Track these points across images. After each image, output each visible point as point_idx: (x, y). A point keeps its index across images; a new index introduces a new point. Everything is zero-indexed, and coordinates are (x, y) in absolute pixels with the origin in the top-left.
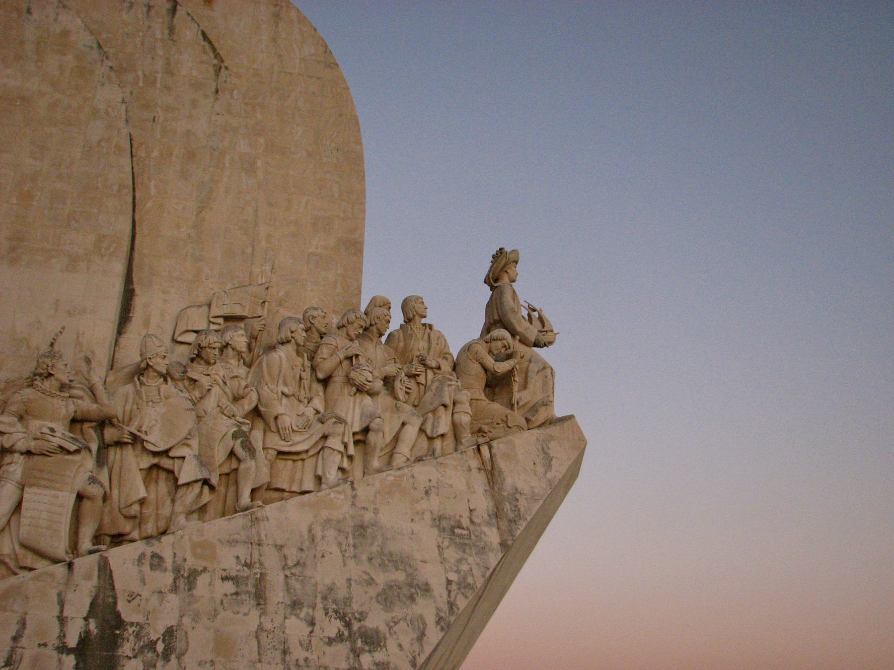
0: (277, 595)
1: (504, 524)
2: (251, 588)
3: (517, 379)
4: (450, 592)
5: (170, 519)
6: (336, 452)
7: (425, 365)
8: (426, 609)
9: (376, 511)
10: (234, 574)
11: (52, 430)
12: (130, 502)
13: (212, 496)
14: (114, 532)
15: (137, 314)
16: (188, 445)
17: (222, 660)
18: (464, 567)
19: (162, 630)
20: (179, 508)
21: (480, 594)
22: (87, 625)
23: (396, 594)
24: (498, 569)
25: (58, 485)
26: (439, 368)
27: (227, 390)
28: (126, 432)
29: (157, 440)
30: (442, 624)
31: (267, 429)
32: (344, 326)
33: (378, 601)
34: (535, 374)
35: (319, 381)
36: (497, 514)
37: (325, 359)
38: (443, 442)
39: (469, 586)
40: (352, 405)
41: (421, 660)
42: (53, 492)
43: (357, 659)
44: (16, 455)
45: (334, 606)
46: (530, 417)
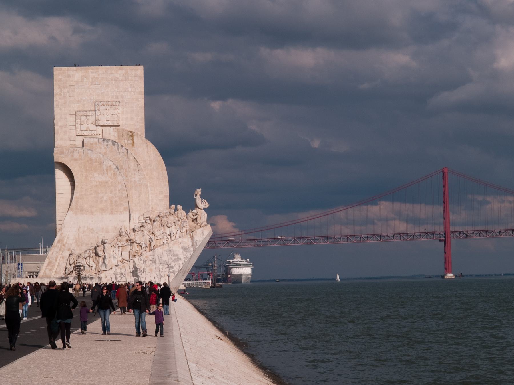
0: (158, 262)
1: (194, 247)
2: (154, 262)
4: (184, 259)
7: (181, 219)
8: (180, 262)
9: (172, 247)
10: (151, 260)
11: (124, 243)
14: (134, 255)
15: (132, 218)
19: (143, 269)
20: (143, 251)
31: (155, 236)
36: (193, 245)
39: (187, 258)
41: (179, 270)
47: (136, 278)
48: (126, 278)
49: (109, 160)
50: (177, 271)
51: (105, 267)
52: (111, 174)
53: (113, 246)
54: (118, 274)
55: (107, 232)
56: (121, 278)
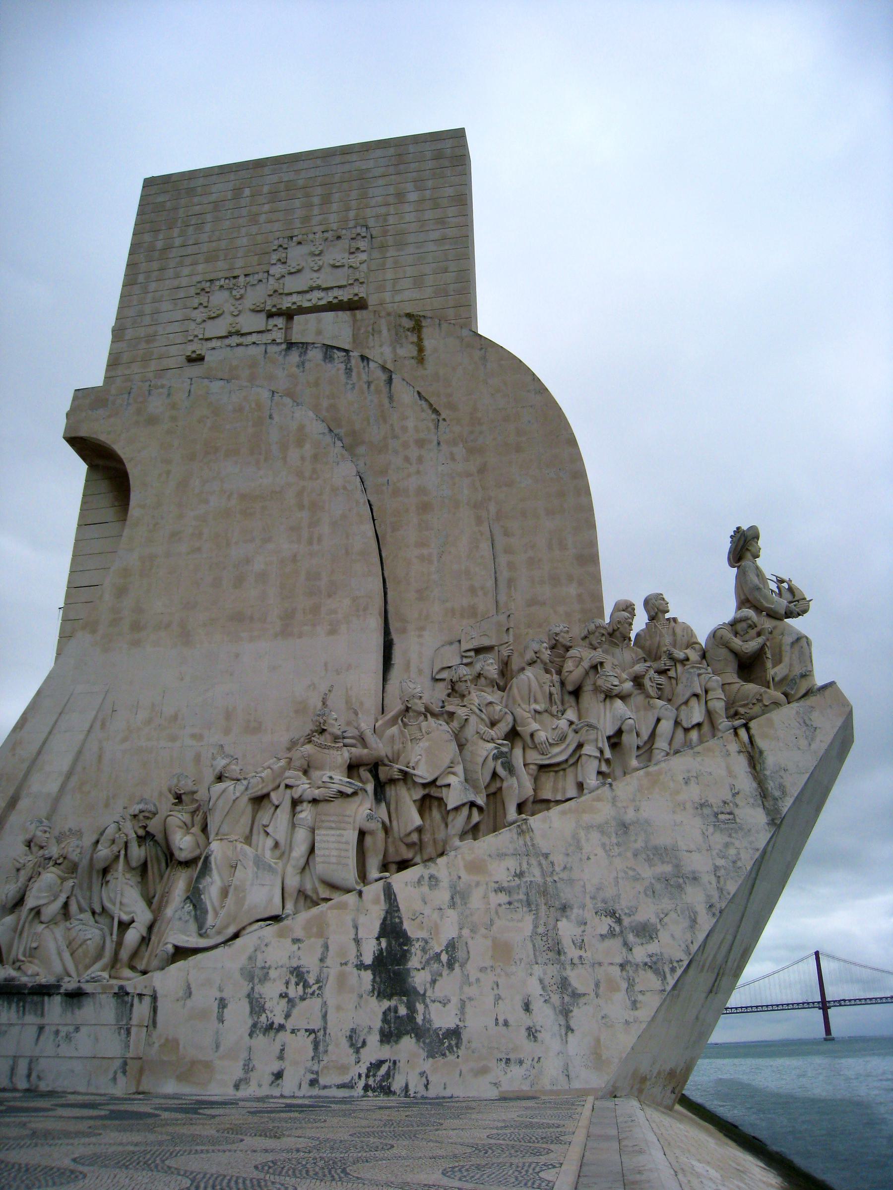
1: (769, 804)
2: (522, 896)
3: (769, 656)
5: (445, 842)
6: (592, 759)
8: (695, 897)
9: (637, 810)
10: (505, 884)
11: (331, 778)
12: (408, 830)
13: (482, 817)
14: (398, 859)
16: (454, 774)
17: (500, 964)
18: (732, 852)
21: (753, 875)
22: (380, 944)
23: (663, 886)
24: (770, 848)
25: (343, 825)
26: (687, 659)
27: (483, 716)
28: (396, 770)
29: (423, 773)
30: (714, 910)
32: (586, 637)
33: (646, 895)
34: (788, 648)
35: (570, 693)
37: (571, 672)
38: (700, 730)
40: (602, 711)
41: (694, 948)
42: (338, 832)
43: (630, 952)
44: (305, 804)
45: (603, 905)
46: (789, 690)
47: (396, 1011)
48: (325, 1003)
49: (298, 405)
50: (679, 954)
51: (193, 926)
52: (303, 459)
53: (267, 796)
54: (273, 974)
55: (254, 728)
56: (290, 1001)
